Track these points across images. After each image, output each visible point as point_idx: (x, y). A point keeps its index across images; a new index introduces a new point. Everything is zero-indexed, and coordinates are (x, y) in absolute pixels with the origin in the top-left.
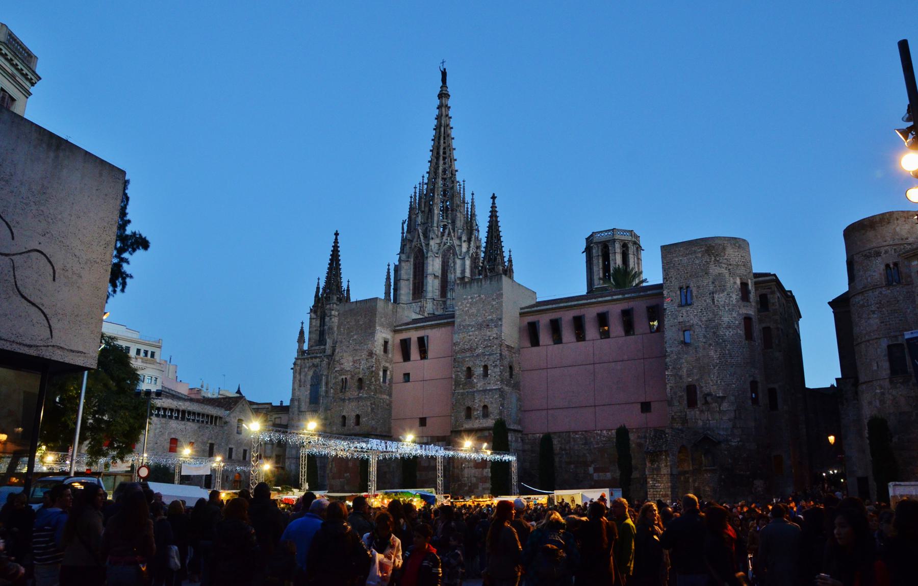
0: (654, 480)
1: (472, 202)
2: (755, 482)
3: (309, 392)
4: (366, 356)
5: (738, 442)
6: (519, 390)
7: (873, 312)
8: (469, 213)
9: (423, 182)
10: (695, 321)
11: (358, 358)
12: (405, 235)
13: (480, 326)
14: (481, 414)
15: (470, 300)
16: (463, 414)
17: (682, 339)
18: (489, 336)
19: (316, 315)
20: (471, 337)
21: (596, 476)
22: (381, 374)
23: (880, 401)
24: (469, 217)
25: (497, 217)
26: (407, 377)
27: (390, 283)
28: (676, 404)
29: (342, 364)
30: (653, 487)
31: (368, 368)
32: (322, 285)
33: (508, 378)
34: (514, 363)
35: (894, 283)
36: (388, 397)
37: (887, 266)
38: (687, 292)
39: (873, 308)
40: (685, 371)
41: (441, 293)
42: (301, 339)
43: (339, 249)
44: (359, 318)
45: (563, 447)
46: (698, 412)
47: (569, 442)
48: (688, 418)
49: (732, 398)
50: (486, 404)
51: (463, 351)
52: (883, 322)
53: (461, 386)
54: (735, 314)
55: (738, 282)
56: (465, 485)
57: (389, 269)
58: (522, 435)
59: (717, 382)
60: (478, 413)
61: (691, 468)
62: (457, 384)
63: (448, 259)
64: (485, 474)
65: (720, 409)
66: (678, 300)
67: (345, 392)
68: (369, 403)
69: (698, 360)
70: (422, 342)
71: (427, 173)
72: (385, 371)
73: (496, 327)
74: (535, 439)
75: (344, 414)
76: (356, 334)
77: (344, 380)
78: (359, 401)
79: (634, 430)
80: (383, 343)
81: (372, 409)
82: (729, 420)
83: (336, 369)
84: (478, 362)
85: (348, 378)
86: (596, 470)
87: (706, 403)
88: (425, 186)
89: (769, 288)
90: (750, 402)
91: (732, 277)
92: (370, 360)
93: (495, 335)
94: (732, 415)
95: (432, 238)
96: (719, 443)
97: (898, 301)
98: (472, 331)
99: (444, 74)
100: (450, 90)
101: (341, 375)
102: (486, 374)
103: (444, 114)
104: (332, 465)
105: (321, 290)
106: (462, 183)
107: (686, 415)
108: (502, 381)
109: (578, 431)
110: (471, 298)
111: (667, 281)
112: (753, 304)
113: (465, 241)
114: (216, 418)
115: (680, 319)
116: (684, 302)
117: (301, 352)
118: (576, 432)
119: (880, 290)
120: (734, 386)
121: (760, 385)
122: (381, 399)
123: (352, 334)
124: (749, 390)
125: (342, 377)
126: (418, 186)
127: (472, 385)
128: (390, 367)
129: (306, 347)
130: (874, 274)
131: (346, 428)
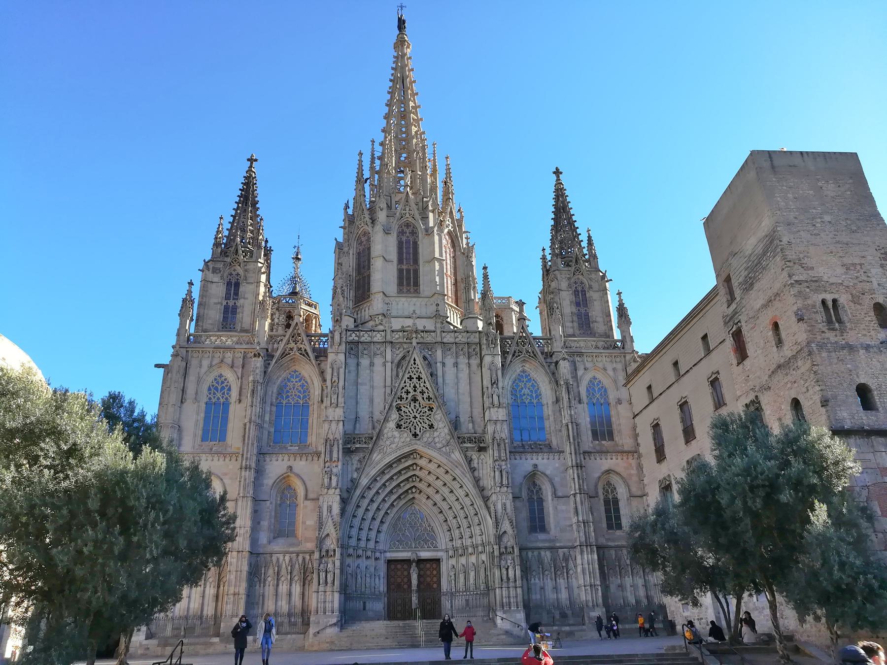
3: (202, 415)
11: (857, 261)
44: (820, 184)
75: (862, 382)
99: (401, 24)
101: (816, 291)
123: (814, 211)
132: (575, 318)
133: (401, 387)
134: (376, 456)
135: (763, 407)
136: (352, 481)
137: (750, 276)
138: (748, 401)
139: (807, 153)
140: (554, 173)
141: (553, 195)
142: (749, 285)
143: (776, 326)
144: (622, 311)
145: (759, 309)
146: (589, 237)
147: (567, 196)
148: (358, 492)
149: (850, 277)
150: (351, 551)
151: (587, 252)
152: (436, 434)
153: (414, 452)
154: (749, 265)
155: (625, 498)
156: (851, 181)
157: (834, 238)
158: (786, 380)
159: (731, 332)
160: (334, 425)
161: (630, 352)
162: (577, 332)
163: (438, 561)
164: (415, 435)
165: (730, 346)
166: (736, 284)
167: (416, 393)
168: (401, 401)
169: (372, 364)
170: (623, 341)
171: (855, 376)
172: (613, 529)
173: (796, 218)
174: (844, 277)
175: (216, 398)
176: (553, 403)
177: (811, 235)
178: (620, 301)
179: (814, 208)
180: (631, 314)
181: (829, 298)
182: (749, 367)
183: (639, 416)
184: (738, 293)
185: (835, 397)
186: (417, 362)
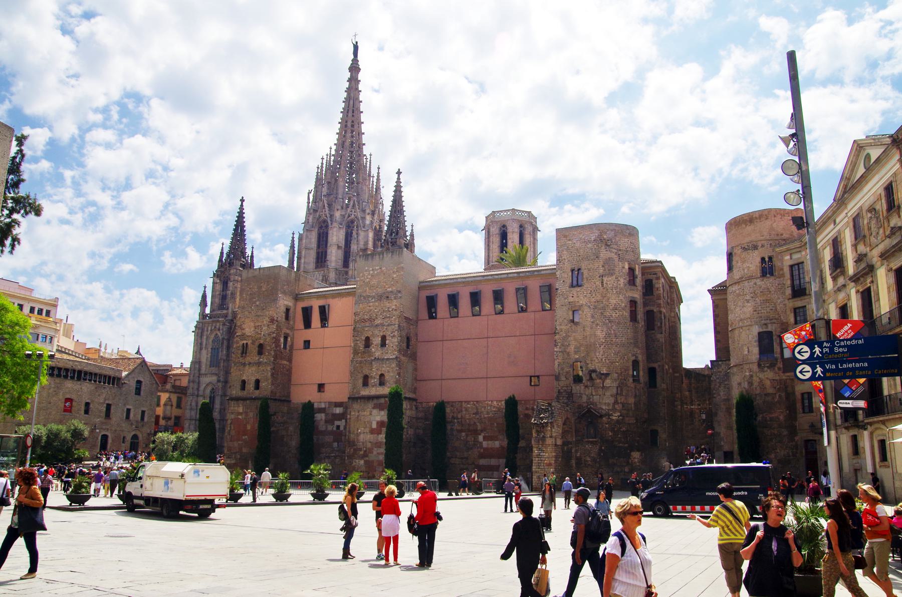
0: (539, 449)
1: (378, 176)
2: (633, 454)
3: (210, 355)
5: (619, 416)
6: (416, 360)
7: (748, 301)
8: (375, 187)
9: (330, 154)
10: (583, 301)
11: (260, 324)
12: (310, 204)
13: (380, 298)
14: (378, 382)
15: (371, 272)
16: (360, 381)
17: (571, 318)
18: (389, 308)
20: (371, 308)
21: (485, 444)
22: (282, 340)
23: (749, 383)
24: (374, 190)
25: (401, 192)
26: (307, 344)
27: (294, 251)
28: (563, 378)
29: (244, 329)
30: (538, 456)
31: (269, 335)
32: (226, 250)
33: (405, 348)
34: (411, 335)
35: (768, 275)
36: (288, 363)
37: (763, 259)
38: (578, 274)
39: (748, 297)
40: (572, 347)
41: (344, 264)
42: (203, 303)
43: (244, 215)
45: (455, 415)
46: (583, 387)
47: (462, 411)
48: (573, 392)
49: (615, 375)
50: (383, 373)
51: (364, 321)
52: (756, 311)
53: (360, 355)
54: (621, 297)
55: (627, 266)
56: (360, 450)
57: (293, 238)
58: (417, 403)
59: (602, 360)
60: (374, 381)
61: (574, 439)
62: (356, 352)
63: (352, 230)
64: (380, 439)
65: (603, 385)
66: (569, 281)
67: (245, 357)
68: (269, 368)
69: (585, 338)
70: (323, 311)
71: (335, 144)
72: (286, 338)
73: (395, 298)
74: (429, 407)
75: (244, 378)
76: (258, 300)
79: (523, 402)
80: (285, 310)
81: (272, 375)
82: (611, 396)
83: (237, 334)
84: (376, 332)
85: (249, 343)
86: (485, 438)
87: (591, 379)
88: (332, 158)
89: (654, 274)
90: (631, 380)
91: (621, 261)
92: (271, 326)
93: (394, 307)
94: (615, 391)
95: (338, 210)
96: (601, 416)
97: (770, 292)
98: (372, 302)
99: (356, 48)
100: (361, 64)
101: (242, 340)
102: (383, 344)
103: (354, 87)
104: (230, 427)
105: (225, 256)
106: (368, 157)
107: (571, 390)
108: (400, 351)
109: (470, 401)
110: (373, 270)
111: (560, 262)
112: (640, 288)
113: (368, 214)
114: (114, 378)
115: (571, 300)
116: (575, 283)
117: (203, 315)
118: (468, 402)
119: (755, 280)
120: (617, 364)
121: (641, 364)
122: (281, 364)
124: (631, 367)
125: (243, 342)
126: (325, 157)
127: (370, 354)
128: (291, 334)
129: (208, 311)
130: (750, 266)
131: (245, 392)
181: (245, 342)
185: (233, 385)
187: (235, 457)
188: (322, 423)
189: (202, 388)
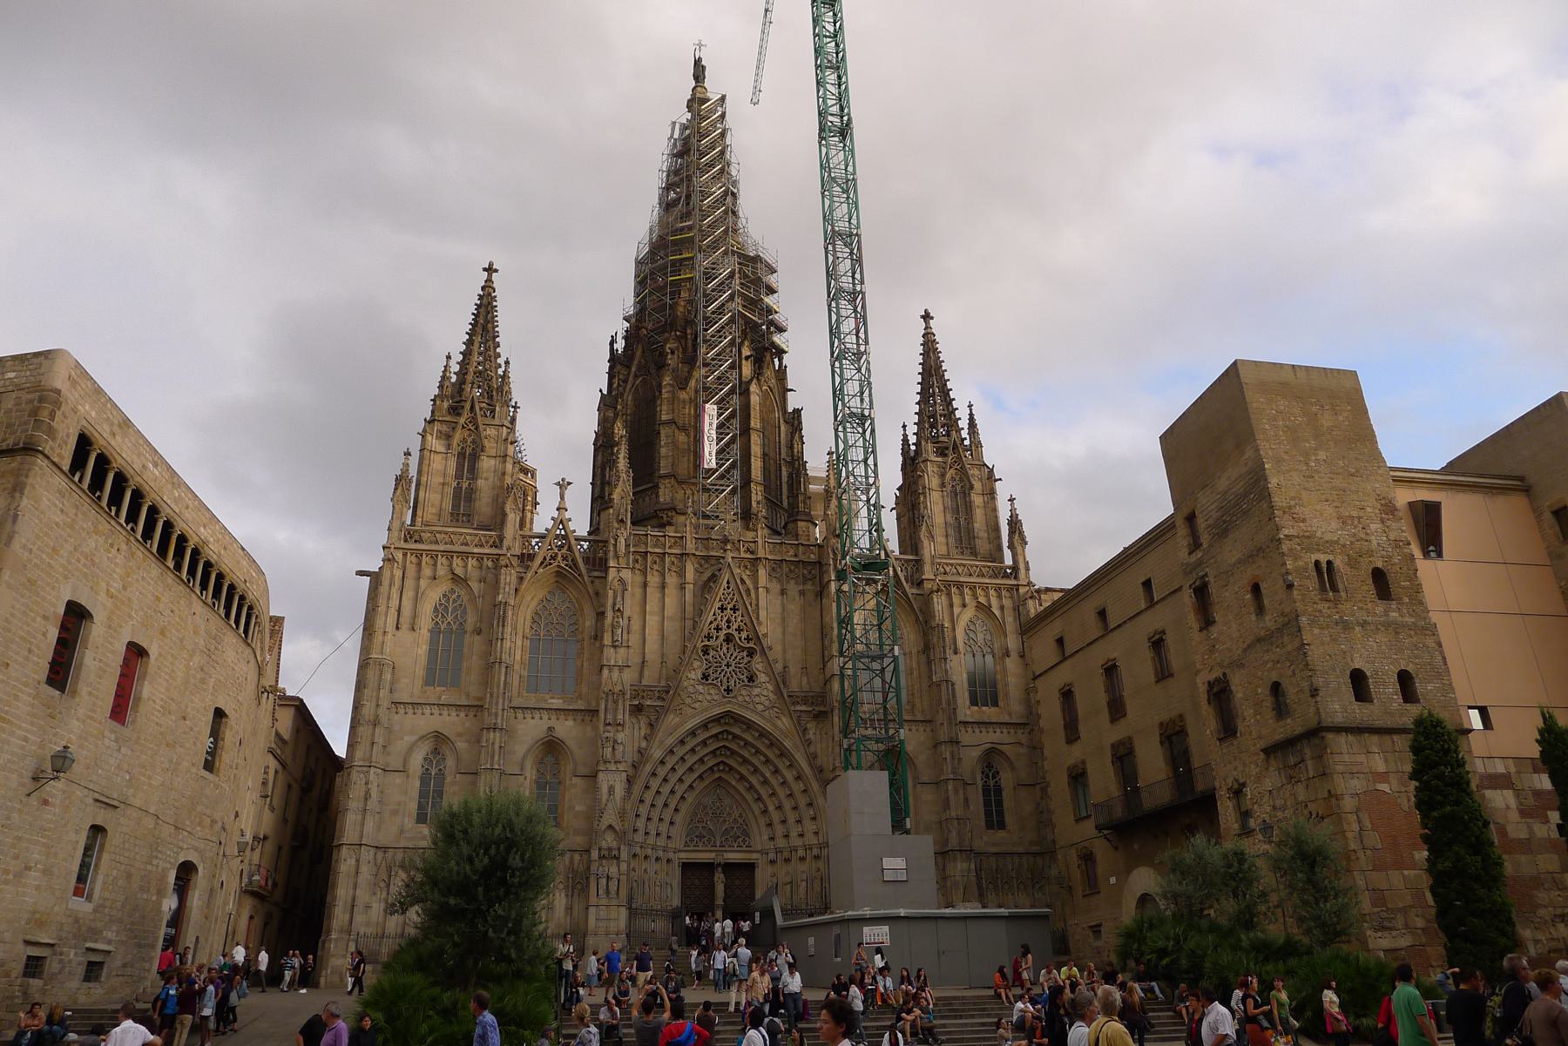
4: (1377, 511)
11: (1354, 513)
19: (449, 446)
44: (1314, 409)
77: (1324, 566)
78: (1397, 633)
101: (1309, 550)
123: (1307, 445)
125: (1314, 557)
132: (951, 531)
133: (709, 621)
134: (671, 719)
135: (1233, 688)
136: (639, 751)
137: (1224, 518)
138: (1212, 677)
139: (1299, 366)
140: (922, 317)
141: (921, 349)
142: (1223, 530)
143: (1256, 589)
144: (1015, 524)
145: (1235, 564)
146: (971, 416)
147: (940, 352)
148: (648, 768)
149: (1347, 533)
150: (638, 850)
151: (968, 437)
152: (756, 691)
153: (728, 714)
154: (1224, 504)
155: (1012, 787)
156: (1349, 408)
157: (1329, 482)
158: (1266, 658)
159: (1193, 587)
160: (615, 674)
161: (1025, 584)
162: (954, 551)
163: (751, 867)
164: (728, 690)
165: (1190, 604)
166: (1203, 526)
167: (730, 631)
168: (709, 641)
169: (663, 586)
170: (1015, 568)
171: (1349, 659)
172: (994, 829)
173: (1287, 453)
174: (1340, 532)
175: (445, 624)
176: (918, 652)
177: (1304, 476)
178: (1013, 510)
179: (1307, 441)
180: (1027, 529)
181: (1323, 558)
182: (1215, 635)
183: (1041, 678)
184: (1205, 539)
186: (732, 586)
187: (1407, 926)
188: (1514, 816)
189: (401, 745)
